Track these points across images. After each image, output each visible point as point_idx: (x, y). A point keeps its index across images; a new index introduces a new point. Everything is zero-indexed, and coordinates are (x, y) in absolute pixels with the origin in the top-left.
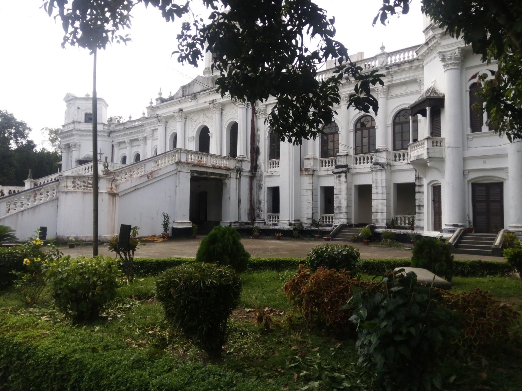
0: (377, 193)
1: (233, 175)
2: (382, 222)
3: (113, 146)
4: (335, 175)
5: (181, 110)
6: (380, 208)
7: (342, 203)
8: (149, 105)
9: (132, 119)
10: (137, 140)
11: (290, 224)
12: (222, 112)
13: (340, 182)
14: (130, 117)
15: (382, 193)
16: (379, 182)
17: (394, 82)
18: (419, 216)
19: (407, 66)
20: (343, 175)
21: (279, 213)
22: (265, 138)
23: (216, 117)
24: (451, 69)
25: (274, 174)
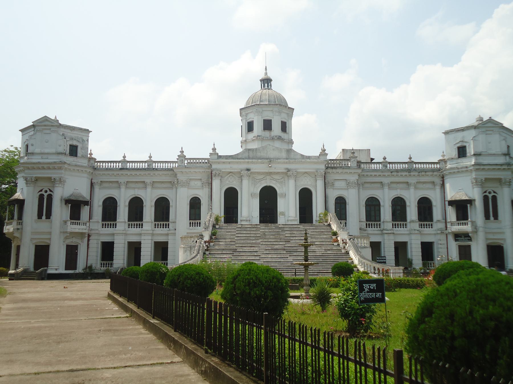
3: (92, 185)
5: (248, 170)
9: (127, 159)
14: (124, 157)
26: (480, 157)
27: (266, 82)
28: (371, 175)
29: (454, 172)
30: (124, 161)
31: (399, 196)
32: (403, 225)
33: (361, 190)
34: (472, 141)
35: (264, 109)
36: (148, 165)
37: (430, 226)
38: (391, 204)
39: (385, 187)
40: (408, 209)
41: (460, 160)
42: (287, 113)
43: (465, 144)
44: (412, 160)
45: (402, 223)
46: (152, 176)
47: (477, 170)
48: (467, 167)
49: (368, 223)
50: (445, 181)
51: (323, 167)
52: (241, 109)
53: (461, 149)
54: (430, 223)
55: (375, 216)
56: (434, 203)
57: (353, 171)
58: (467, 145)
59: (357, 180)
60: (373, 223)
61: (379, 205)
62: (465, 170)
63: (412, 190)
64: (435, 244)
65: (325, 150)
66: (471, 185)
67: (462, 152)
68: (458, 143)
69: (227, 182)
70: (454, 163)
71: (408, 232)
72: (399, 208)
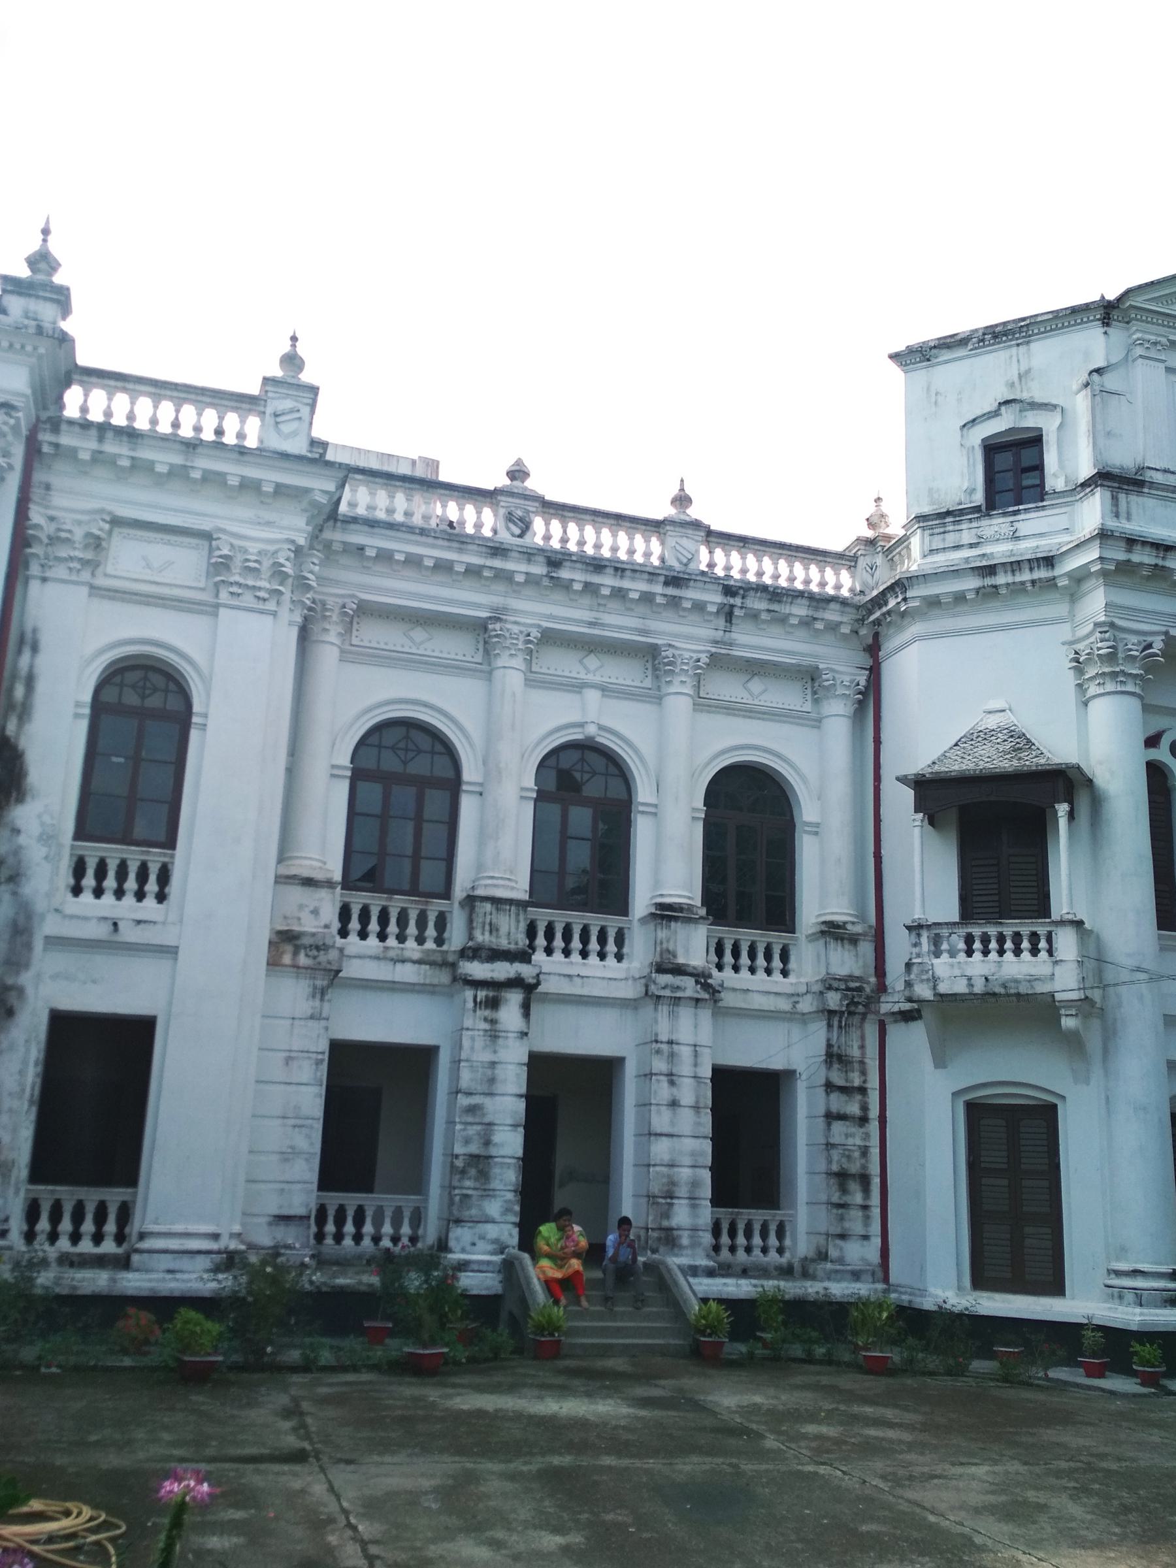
0: (674, 1104)
2: (694, 1245)
4: (469, 994)
6: (685, 1173)
7: (497, 1138)
11: (229, 1261)
13: (494, 1034)
15: (696, 1108)
16: (685, 1052)
17: (737, 653)
18: (841, 1218)
19: (800, 610)
20: (514, 998)
21: (130, 1177)
24: (1109, 693)
25: (129, 934)
26: (1134, 502)
28: (413, 561)
29: (960, 598)
31: (591, 730)
32: (602, 939)
33: (327, 655)
34: (1081, 404)
37: (777, 963)
38: (530, 781)
40: (643, 831)
41: (997, 525)
43: (1031, 420)
44: (694, 513)
45: (595, 921)
47: (1119, 574)
48: (1049, 561)
49: (357, 900)
50: (889, 671)
53: (1004, 460)
54: (777, 939)
55: (416, 858)
56: (808, 811)
57: (271, 476)
58: (1048, 424)
59: (298, 551)
60: (396, 904)
61: (453, 785)
62: (1039, 579)
63: (678, 703)
64: (801, 1087)
65: (42, 261)
66: (1070, 679)
67: (1013, 468)
68: (995, 414)
70: (951, 539)
71: (629, 991)
72: (581, 818)
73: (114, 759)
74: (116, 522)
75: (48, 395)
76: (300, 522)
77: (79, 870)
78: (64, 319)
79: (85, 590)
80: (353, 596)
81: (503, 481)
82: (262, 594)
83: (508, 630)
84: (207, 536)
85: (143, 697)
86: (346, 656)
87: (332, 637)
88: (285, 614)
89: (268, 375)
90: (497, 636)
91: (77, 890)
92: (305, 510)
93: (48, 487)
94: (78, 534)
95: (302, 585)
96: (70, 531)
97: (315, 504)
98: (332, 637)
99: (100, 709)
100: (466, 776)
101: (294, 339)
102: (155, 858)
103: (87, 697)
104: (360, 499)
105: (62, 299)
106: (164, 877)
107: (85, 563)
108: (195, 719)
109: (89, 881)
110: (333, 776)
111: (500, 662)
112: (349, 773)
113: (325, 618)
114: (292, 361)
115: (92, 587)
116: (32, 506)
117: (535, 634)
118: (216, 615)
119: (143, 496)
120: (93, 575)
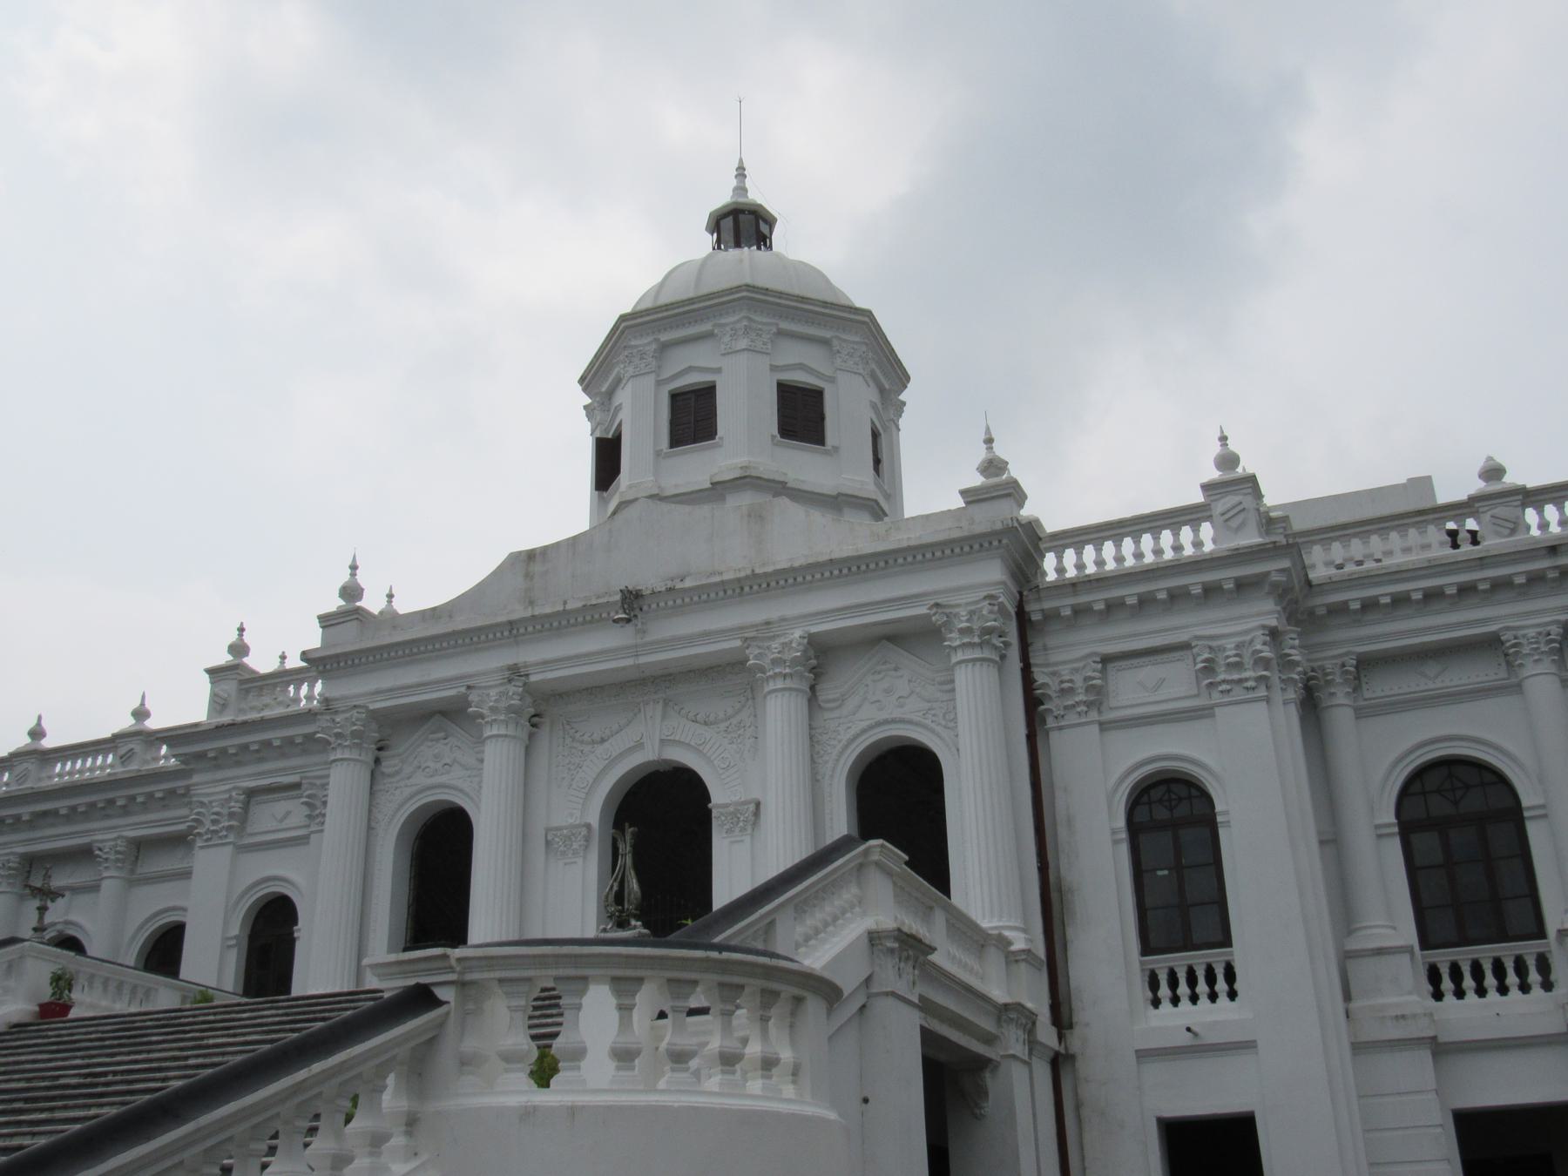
1: (1013, 1041)
5: (515, 672)
8: (224, 658)
9: (48, 743)
10: (84, 855)
12: (812, 688)
14: (37, 733)
22: (1114, 832)
23: (780, 712)
27: (743, 225)
28: (1400, 601)
30: (37, 756)
35: (664, 337)
36: (125, 759)
39: (1530, 669)
42: (825, 342)
46: (126, 811)
51: (991, 574)
52: (581, 381)
59: (1274, 634)
60: (1486, 953)
61: (1512, 815)
65: (993, 466)
69: (421, 780)
73: (1160, 873)
74: (1106, 660)
75: (1024, 568)
76: (1269, 605)
77: (1154, 984)
78: (1021, 505)
79: (1096, 728)
80: (1346, 654)
81: (1477, 486)
82: (1249, 684)
83: (1524, 636)
84: (1185, 646)
85: (1171, 810)
86: (1360, 713)
87: (1341, 699)
88: (1278, 697)
89: (1205, 480)
90: (1514, 646)
91: (1156, 1003)
92: (1269, 593)
93: (1045, 648)
94: (1079, 683)
95: (1286, 663)
96: (1071, 681)
97: (1275, 585)
98: (1341, 699)
99: (1136, 829)
100: (1525, 802)
101: (1223, 439)
102: (1216, 957)
103: (1121, 822)
104: (1321, 564)
105: (1014, 493)
106: (1230, 976)
107: (1089, 704)
108: (1219, 819)
109: (1164, 991)
110: (1380, 836)
111: (1525, 672)
112: (1396, 830)
113: (1329, 683)
114: (1228, 460)
115: (1101, 724)
116: (1034, 669)
117: (1555, 631)
118: (1213, 716)
119: (1126, 628)
120: (1100, 712)
